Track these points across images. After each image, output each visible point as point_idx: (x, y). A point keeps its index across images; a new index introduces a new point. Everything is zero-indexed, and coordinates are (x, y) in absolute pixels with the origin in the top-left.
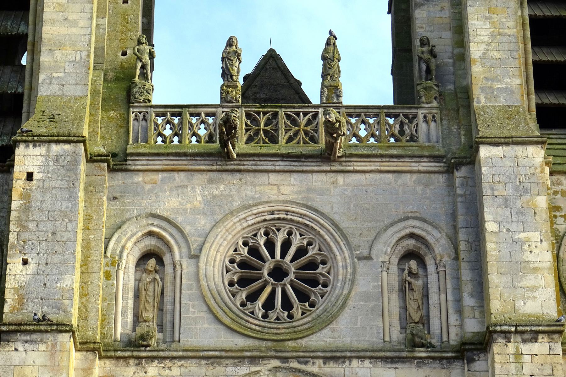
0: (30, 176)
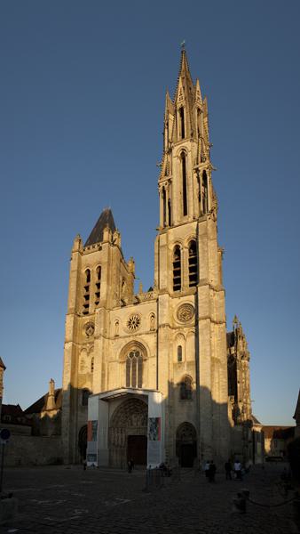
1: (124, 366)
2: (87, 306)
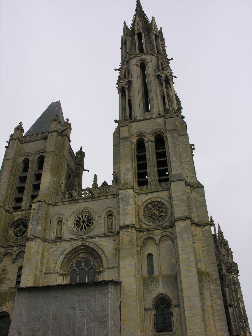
0: (34, 209)
2: (19, 200)
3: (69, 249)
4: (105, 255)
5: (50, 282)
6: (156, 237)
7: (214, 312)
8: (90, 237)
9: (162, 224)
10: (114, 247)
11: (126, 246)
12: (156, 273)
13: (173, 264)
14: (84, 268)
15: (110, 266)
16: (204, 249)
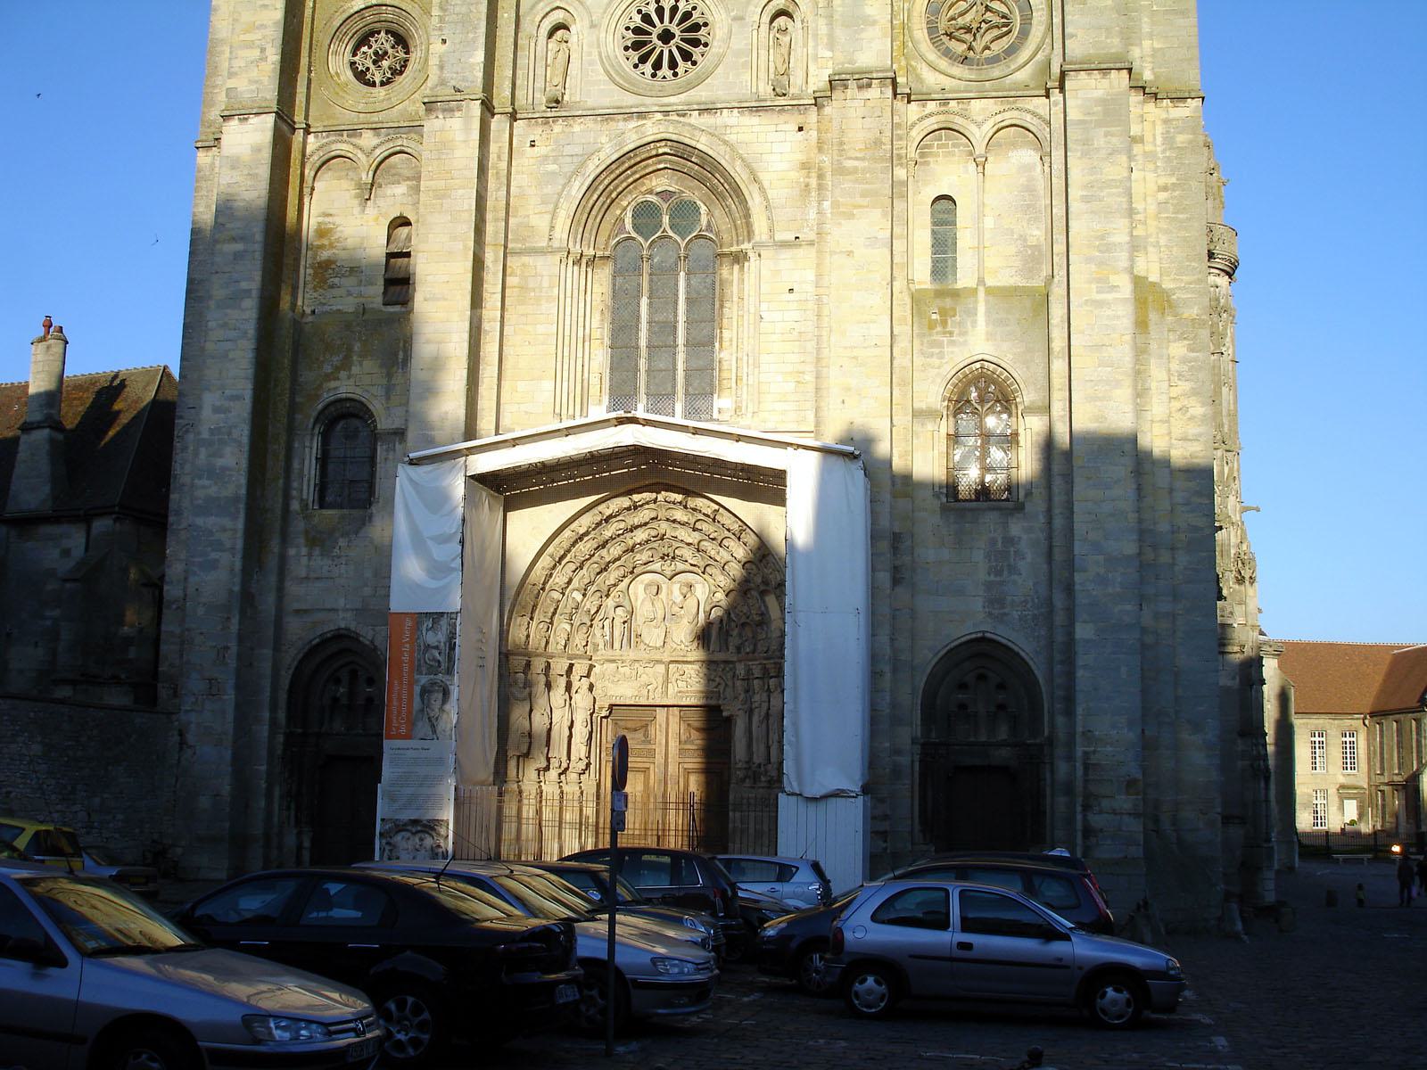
1: (602, 280)
3: (608, 153)
4: (762, 190)
5: (534, 290)
6: (973, 128)
7: (1174, 441)
8: (696, 107)
9: (1002, 74)
10: (801, 157)
11: (856, 163)
12: (965, 278)
13: (1036, 246)
14: (671, 237)
15: (779, 237)
16: (1163, 196)
